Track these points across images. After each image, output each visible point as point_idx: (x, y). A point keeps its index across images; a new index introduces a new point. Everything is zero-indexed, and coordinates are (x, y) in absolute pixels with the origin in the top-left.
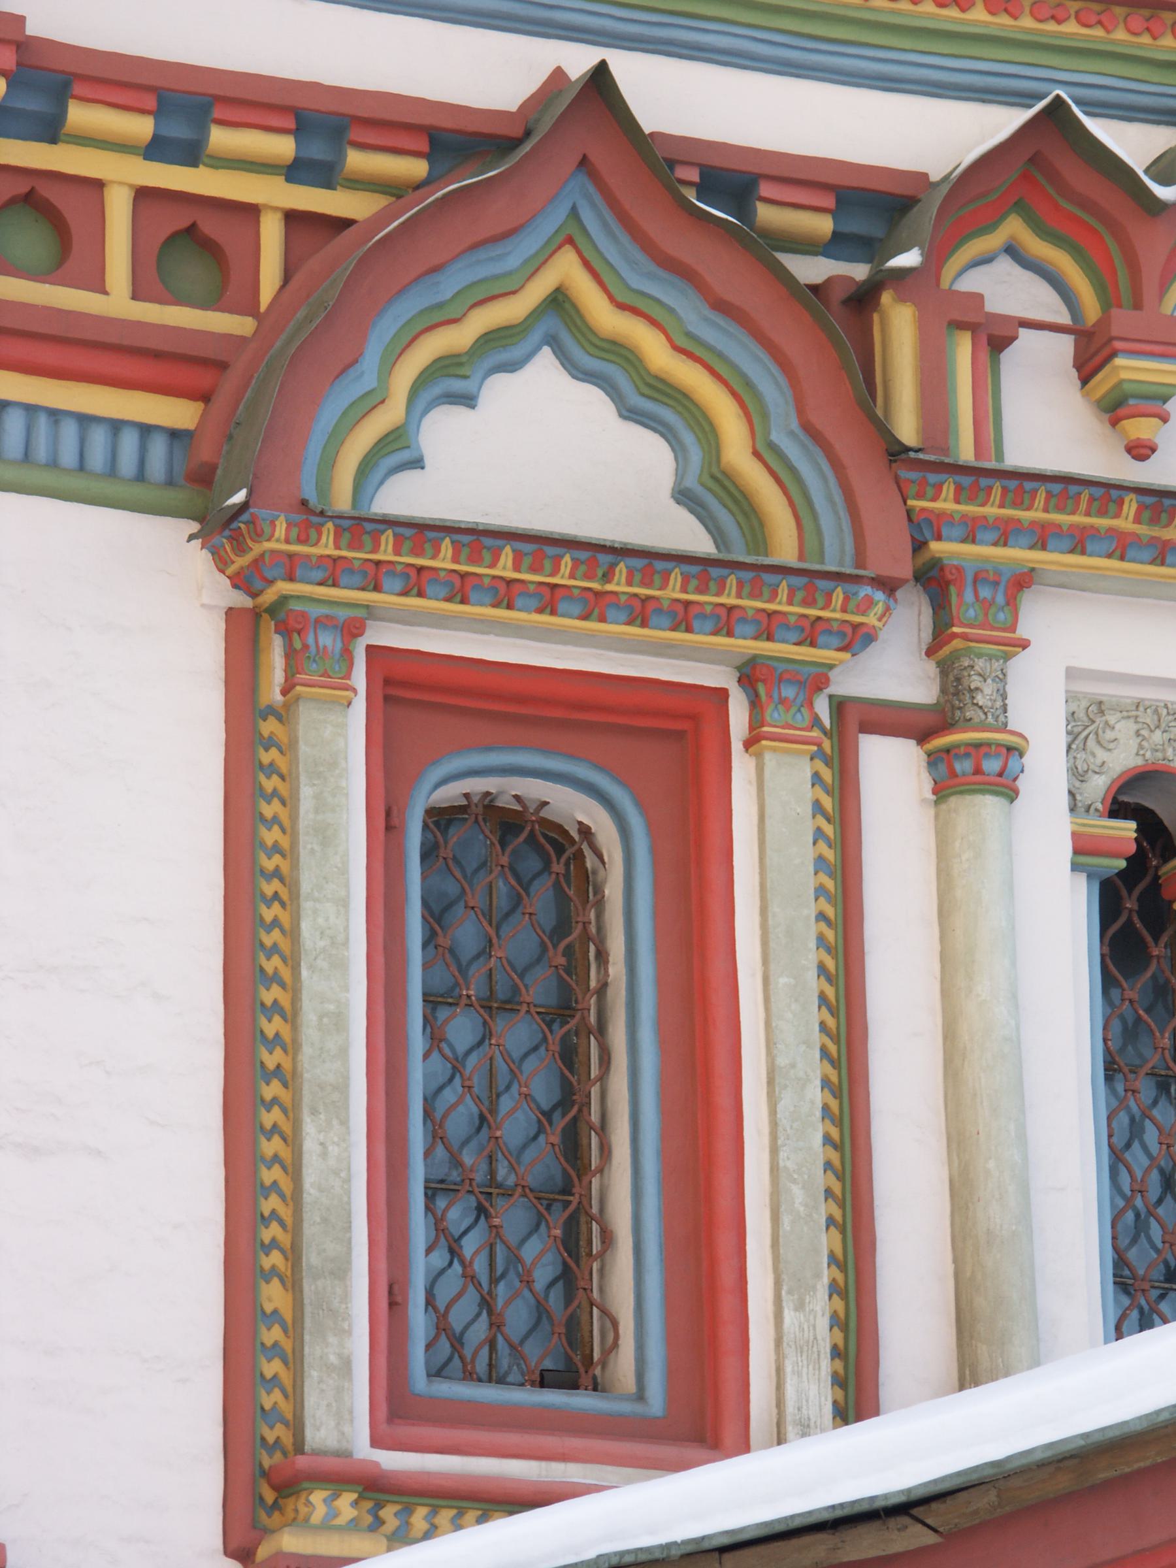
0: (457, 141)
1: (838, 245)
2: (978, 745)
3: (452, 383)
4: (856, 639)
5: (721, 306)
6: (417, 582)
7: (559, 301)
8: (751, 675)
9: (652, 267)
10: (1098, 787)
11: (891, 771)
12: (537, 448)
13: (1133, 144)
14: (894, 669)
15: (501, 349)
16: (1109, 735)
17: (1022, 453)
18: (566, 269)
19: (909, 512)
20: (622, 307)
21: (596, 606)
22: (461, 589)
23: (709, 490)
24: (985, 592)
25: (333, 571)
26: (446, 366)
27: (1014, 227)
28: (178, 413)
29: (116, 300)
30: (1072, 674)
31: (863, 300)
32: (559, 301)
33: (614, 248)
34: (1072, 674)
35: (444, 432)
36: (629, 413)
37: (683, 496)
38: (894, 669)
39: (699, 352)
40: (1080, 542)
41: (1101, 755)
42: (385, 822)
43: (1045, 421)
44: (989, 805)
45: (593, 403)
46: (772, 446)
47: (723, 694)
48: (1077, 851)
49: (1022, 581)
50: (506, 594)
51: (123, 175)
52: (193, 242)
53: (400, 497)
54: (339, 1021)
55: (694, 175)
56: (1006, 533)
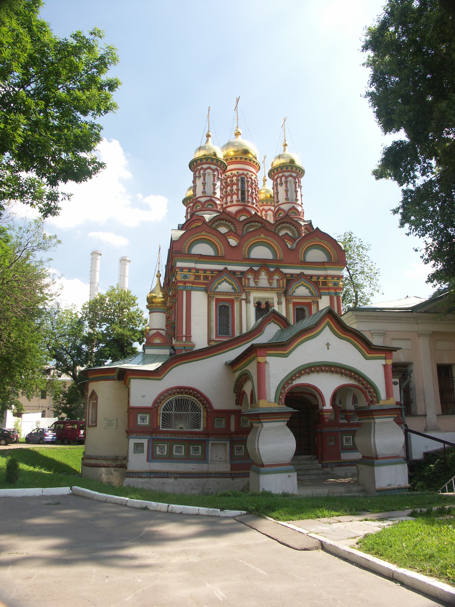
0: (220, 271)
1: (241, 275)
3: (220, 284)
4: (241, 296)
6: (217, 294)
7: (225, 279)
8: (236, 298)
10: (255, 302)
11: (244, 302)
12: (225, 287)
13: (256, 269)
14: (244, 297)
15: (222, 282)
18: (225, 277)
21: (226, 295)
22: (219, 295)
25: (212, 294)
26: (219, 283)
28: (205, 286)
29: (202, 281)
32: (225, 279)
33: (228, 276)
35: (219, 286)
38: (244, 297)
40: (253, 290)
42: (216, 307)
44: (248, 304)
49: (250, 292)
50: (222, 295)
51: (202, 275)
52: (206, 278)
53: (217, 290)
54: (213, 317)
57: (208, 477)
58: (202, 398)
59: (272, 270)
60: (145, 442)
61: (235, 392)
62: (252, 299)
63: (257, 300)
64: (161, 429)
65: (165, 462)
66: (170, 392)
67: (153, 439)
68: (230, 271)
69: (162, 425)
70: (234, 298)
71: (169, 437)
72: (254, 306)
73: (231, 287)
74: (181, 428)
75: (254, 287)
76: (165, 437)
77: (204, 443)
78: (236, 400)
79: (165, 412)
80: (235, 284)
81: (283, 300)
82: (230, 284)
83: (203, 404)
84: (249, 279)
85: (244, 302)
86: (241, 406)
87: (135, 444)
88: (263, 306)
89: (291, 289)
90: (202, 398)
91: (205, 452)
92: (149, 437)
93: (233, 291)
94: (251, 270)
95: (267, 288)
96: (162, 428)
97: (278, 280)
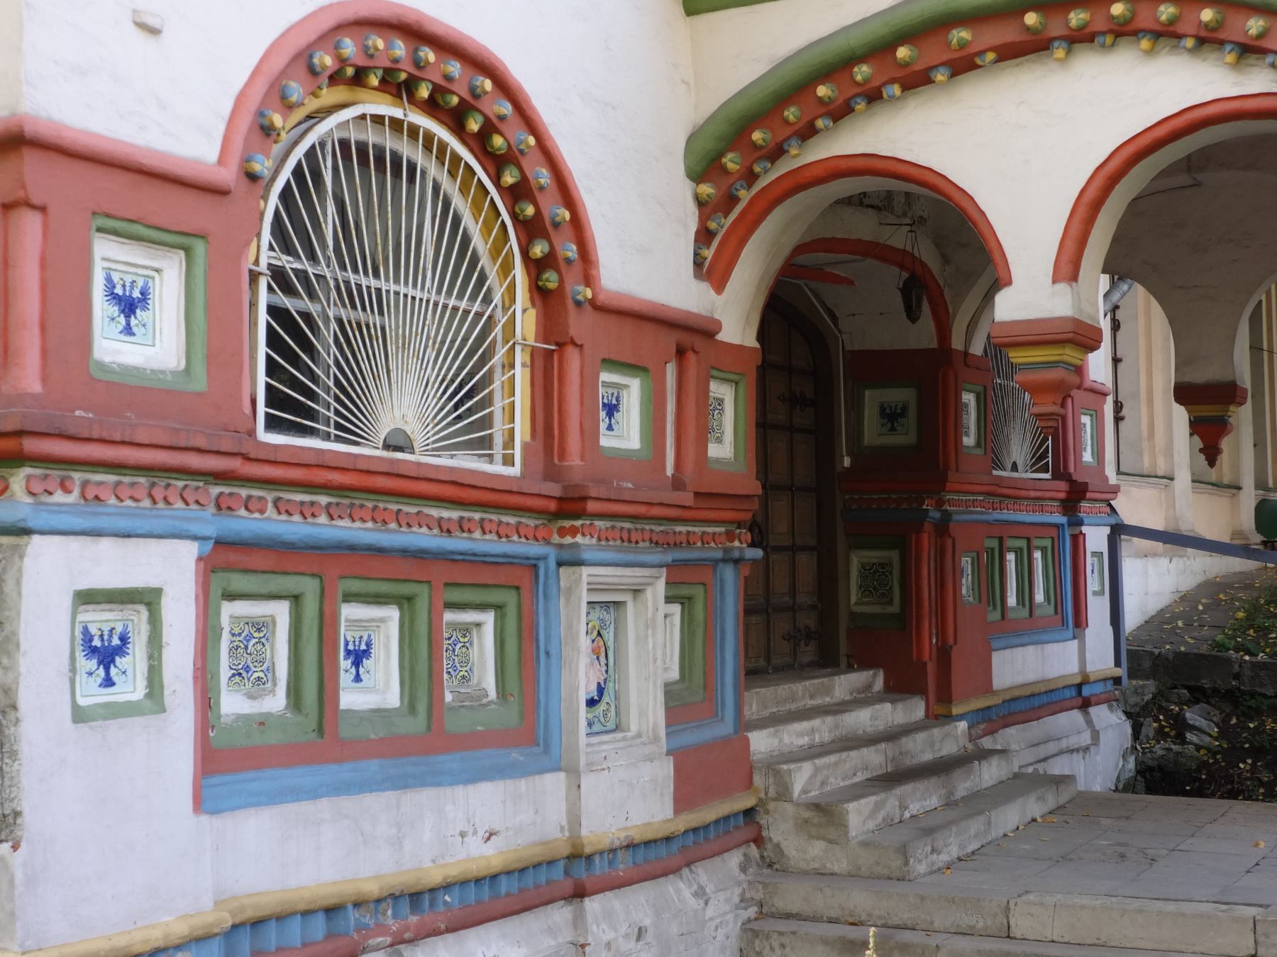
57: (579, 893)
58: (543, 176)
60: (171, 566)
61: (705, 168)
64: (264, 436)
65: (313, 794)
66: (349, 47)
67: (222, 544)
69: (274, 398)
71: (325, 529)
74: (398, 442)
76: (293, 528)
77: (515, 589)
78: (704, 236)
79: (287, 262)
83: (531, 229)
86: (719, 287)
87: (87, 598)
90: (543, 176)
91: (526, 655)
92: (212, 524)
96: (273, 424)
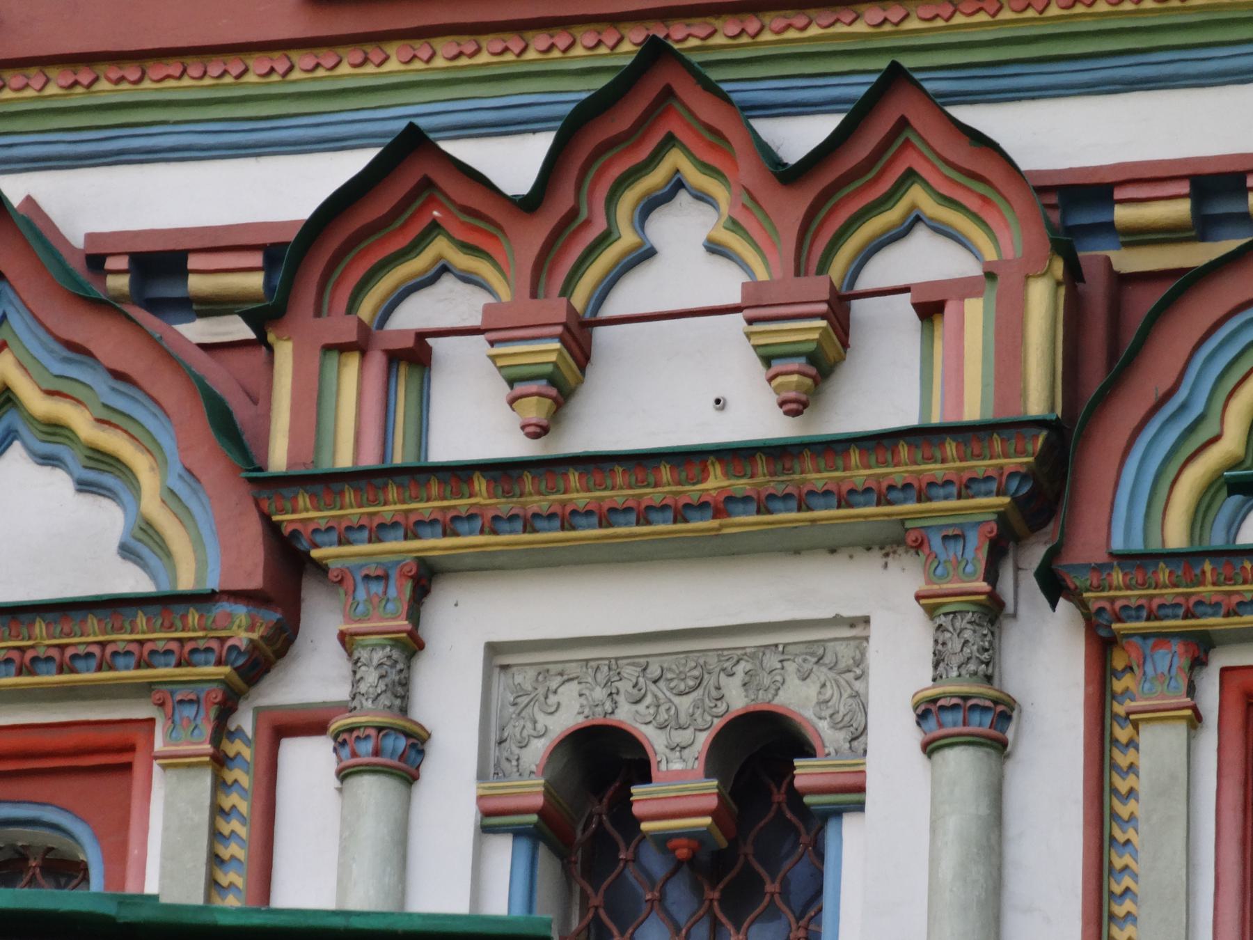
2: (351, 730)
5: (118, 375)
9: (67, 353)
16: (553, 699)
17: (442, 450)
19: (272, 528)
20: (51, 393)
23: (142, 543)
24: (377, 588)
27: (440, 247)
30: (493, 649)
31: (261, 341)
34: (493, 649)
36: (84, 486)
37: (126, 551)
38: (318, 674)
39: (115, 419)
41: (543, 720)
43: (473, 419)
45: (58, 483)
46: (172, 491)
47: (151, 721)
48: (487, 814)
55: (122, 263)
56: (379, 531)
59: (798, 137)
62: (449, 699)
63: (568, 713)
68: (96, 262)
70: (140, 711)
72: (491, 821)
73: (106, 520)
75: (502, 472)
80: (150, 446)
81: (1047, 663)
82: (100, 473)
84: (415, 356)
85: (308, 764)
88: (679, 788)
89: (1160, 439)
93: (131, 581)
94: (407, 188)
95: (736, 456)
97: (930, 310)
